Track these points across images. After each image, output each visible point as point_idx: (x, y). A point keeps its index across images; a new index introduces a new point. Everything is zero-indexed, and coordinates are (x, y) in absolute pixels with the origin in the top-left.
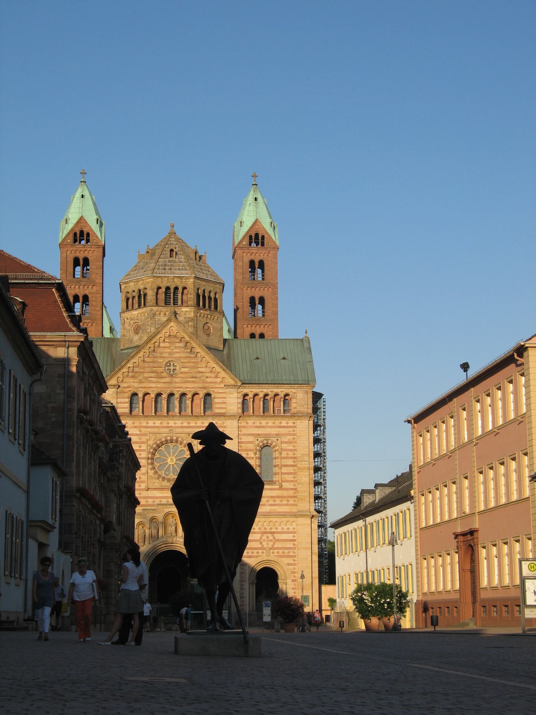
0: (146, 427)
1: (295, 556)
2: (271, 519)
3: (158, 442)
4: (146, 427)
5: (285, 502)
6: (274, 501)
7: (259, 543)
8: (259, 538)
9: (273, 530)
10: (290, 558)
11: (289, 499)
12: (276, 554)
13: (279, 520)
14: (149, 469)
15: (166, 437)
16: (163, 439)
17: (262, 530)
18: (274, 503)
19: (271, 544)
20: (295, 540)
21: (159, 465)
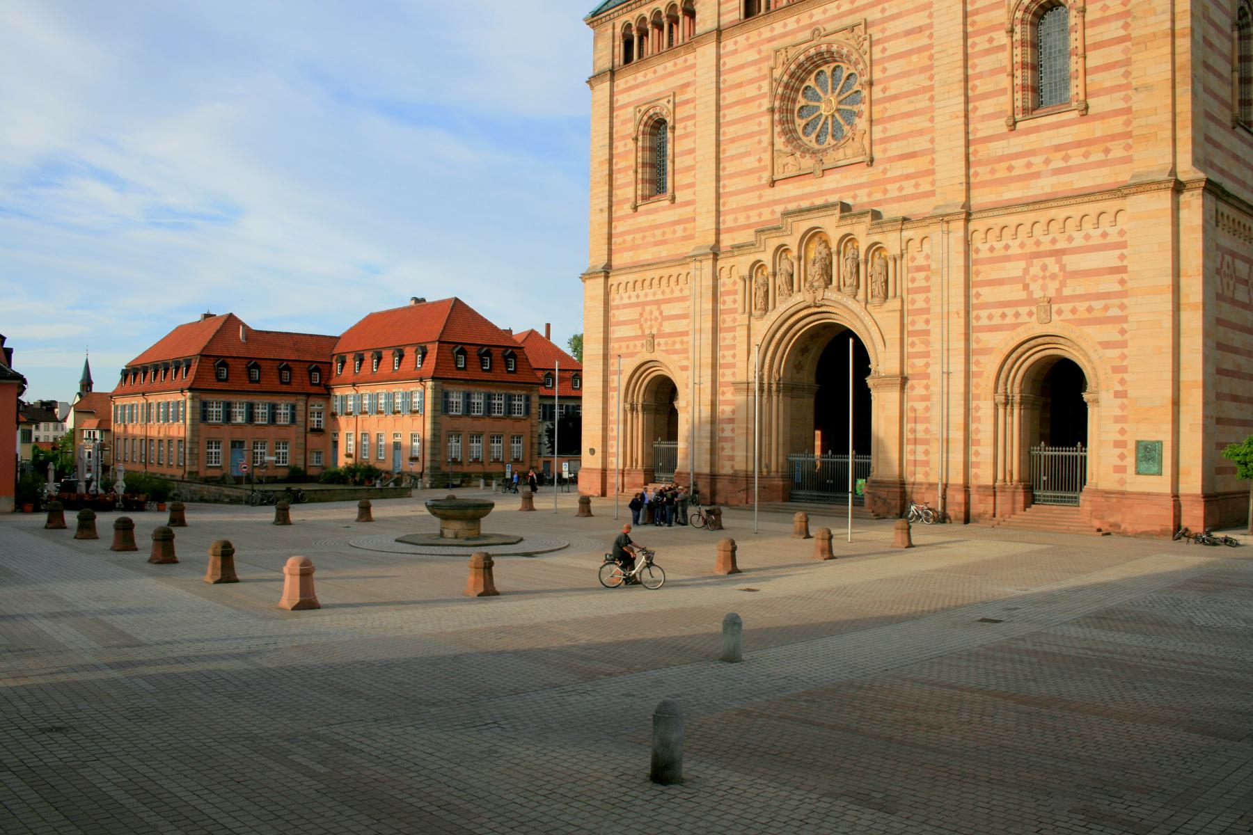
0: (771, 40)
1: (1124, 319)
2: (1053, 213)
3: (793, 67)
4: (771, 40)
5: (1097, 156)
6: (1066, 158)
7: (1021, 286)
8: (1019, 273)
9: (1060, 245)
10: (1110, 326)
11: (1109, 145)
12: (1067, 315)
13: (1075, 211)
14: (775, 135)
15: (806, 50)
16: (802, 58)
17: (1031, 248)
18: (1063, 164)
19: (1053, 286)
20: (1123, 269)
21: (804, 124)
